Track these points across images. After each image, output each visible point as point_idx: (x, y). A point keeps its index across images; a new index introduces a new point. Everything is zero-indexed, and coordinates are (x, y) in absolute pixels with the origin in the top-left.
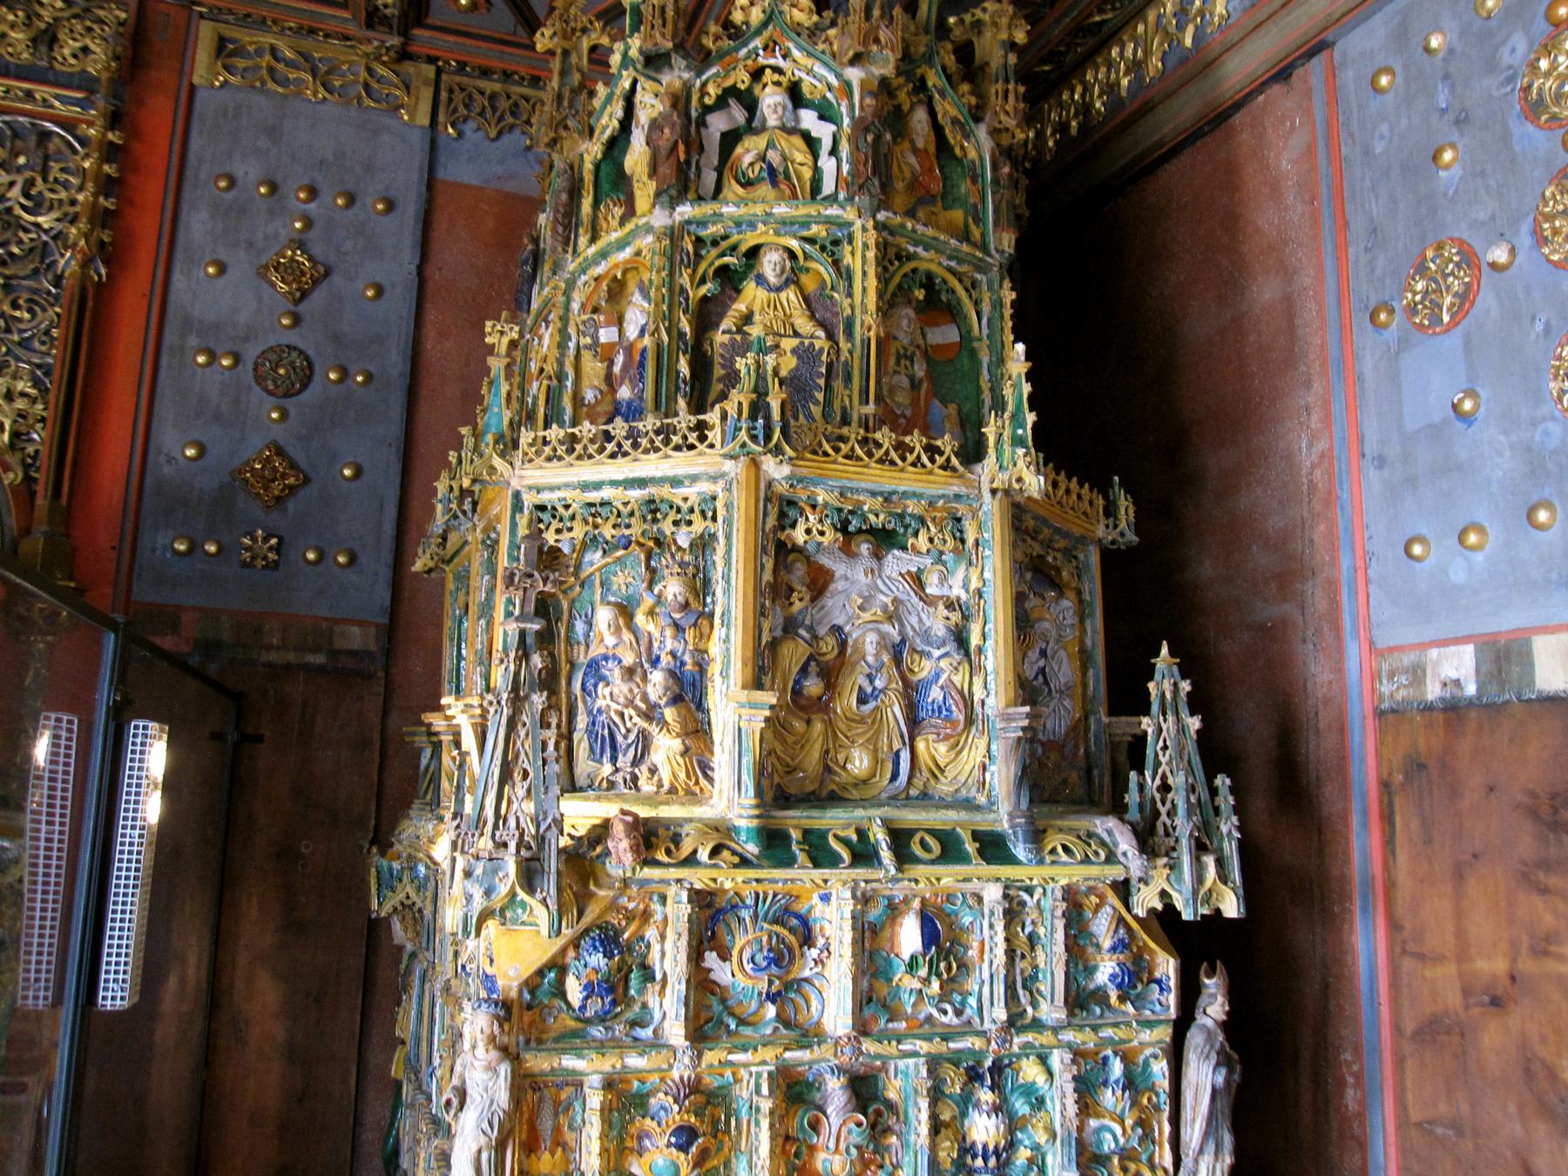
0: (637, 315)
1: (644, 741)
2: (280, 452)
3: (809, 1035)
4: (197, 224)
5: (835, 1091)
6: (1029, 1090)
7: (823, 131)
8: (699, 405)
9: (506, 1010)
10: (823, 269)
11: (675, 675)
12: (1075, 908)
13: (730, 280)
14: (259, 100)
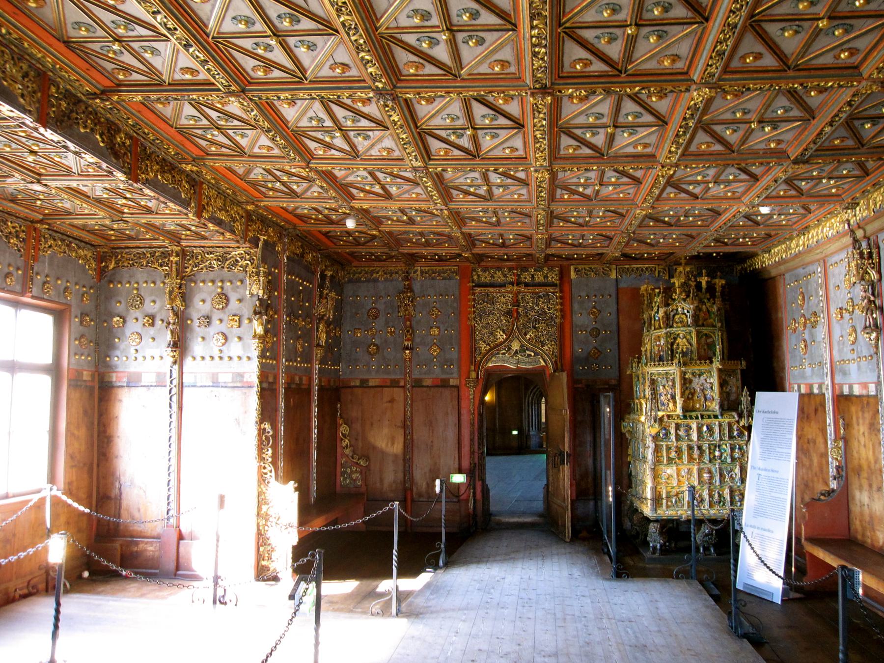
0: (662, 342)
1: (668, 404)
2: (596, 349)
3: (692, 441)
4: (576, 306)
5: (696, 448)
6: (724, 449)
7: (688, 314)
8: (672, 360)
9: (653, 437)
10: (688, 337)
11: (671, 395)
12: (730, 426)
13: (675, 339)
14: (583, 279)
